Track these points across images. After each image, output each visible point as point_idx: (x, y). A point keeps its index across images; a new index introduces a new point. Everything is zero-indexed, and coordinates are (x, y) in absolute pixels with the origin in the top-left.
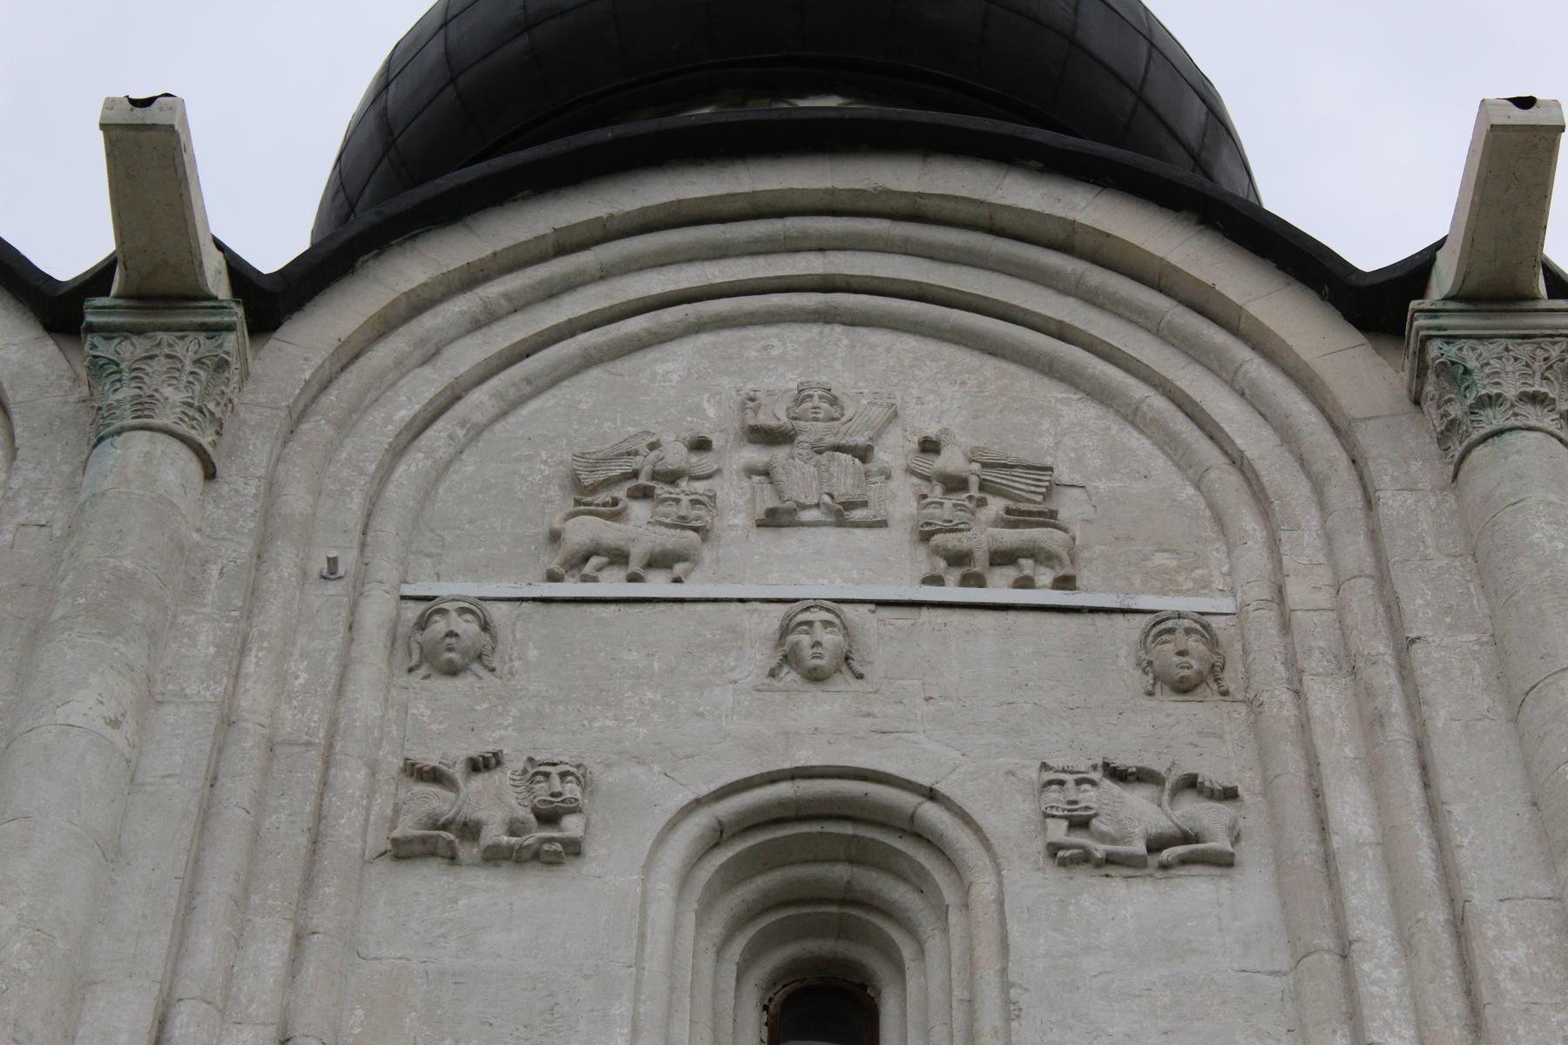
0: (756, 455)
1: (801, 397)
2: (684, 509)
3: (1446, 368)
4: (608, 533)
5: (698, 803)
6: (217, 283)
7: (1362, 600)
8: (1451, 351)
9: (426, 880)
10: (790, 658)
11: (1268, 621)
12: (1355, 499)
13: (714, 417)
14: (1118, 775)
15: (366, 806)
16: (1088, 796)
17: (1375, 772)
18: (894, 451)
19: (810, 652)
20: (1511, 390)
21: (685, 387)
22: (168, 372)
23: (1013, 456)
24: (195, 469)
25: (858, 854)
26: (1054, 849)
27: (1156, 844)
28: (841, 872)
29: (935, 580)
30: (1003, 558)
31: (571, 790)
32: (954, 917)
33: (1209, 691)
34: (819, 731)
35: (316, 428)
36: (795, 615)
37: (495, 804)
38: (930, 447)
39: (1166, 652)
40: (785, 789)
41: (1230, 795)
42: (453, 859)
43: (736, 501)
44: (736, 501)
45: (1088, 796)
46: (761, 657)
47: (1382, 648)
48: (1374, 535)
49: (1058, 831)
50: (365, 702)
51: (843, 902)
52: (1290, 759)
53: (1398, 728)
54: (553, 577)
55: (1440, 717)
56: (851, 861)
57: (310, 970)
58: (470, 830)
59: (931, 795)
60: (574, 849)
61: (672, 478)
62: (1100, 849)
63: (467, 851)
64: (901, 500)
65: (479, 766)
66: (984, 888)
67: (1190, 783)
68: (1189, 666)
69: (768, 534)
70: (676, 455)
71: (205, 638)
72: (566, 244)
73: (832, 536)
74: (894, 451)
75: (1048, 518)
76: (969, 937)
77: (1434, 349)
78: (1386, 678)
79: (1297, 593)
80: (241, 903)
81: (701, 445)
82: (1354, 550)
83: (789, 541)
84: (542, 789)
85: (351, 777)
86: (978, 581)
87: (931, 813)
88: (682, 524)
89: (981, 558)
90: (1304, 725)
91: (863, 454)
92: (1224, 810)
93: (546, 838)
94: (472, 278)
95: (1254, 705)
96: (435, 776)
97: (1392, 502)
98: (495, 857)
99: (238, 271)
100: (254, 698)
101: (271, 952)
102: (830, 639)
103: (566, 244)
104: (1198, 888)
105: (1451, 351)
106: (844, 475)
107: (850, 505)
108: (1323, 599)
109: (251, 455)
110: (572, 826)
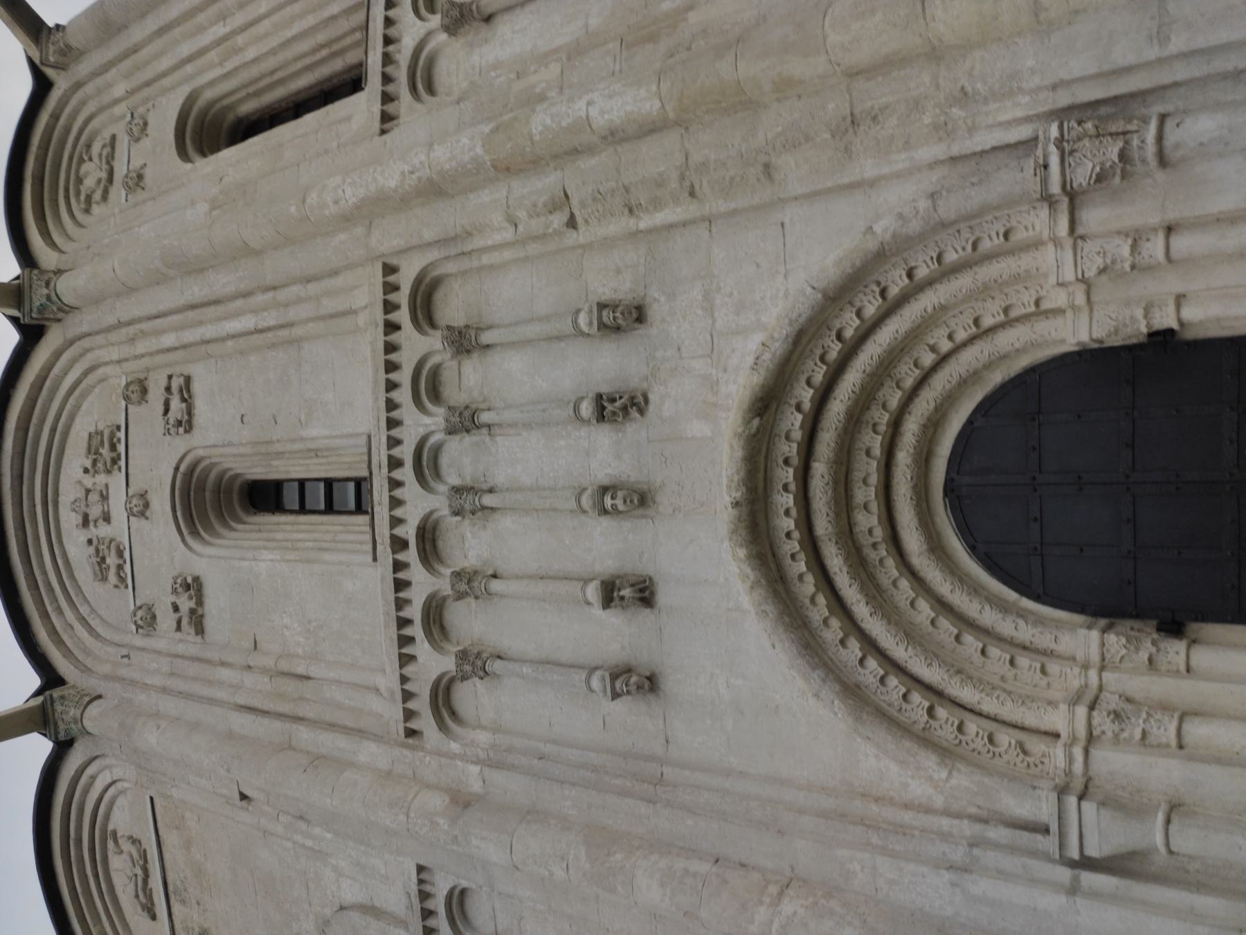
0: (92, 524)
1: (74, 510)
2: (104, 547)
3: (39, 312)
4: (113, 571)
5: (183, 540)
6: (40, 699)
7: (113, 337)
8: (35, 310)
9: (209, 623)
10: (142, 514)
11: (125, 365)
12: (87, 339)
13: (82, 536)
14: (166, 411)
15: (189, 643)
16: (171, 421)
17: (159, 333)
18: (88, 481)
19: (141, 508)
20: (45, 291)
21: (76, 545)
22: (67, 713)
23: (85, 445)
24: (95, 703)
25: (201, 488)
26: (186, 431)
27: (184, 400)
28: (208, 495)
29: (120, 469)
30: (113, 447)
31: (179, 581)
32: (213, 460)
33: (146, 383)
34: (161, 503)
35: (89, 662)
36: (131, 513)
37: (186, 604)
38: (86, 471)
39: (134, 397)
40: (179, 514)
41: (170, 377)
42: (202, 616)
43: (103, 531)
44: (103, 531)
45: (171, 421)
46: (143, 521)
47: (124, 331)
48: (98, 333)
49: (181, 430)
50: (160, 644)
51: (219, 492)
52: (159, 359)
53: (144, 326)
54: (127, 587)
55: (137, 313)
56: (204, 490)
57: (230, 660)
58: (192, 612)
59: (177, 469)
60: (197, 579)
61: (97, 550)
62: (186, 417)
63: (200, 612)
64: (101, 479)
65: (176, 608)
66: (201, 452)
67: (168, 389)
68: (138, 390)
69: (112, 520)
70: (92, 550)
71: (141, 697)
72: (34, 586)
73: (111, 501)
74: (88, 481)
75: (102, 433)
76: (221, 456)
77: (34, 315)
78: (131, 330)
79: (115, 357)
80: (211, 683)
81: (90, 542)
82: (99, 339)
83: (113, 514)
84: (180, 590)
85: (180, 648)
86: (119, 455)
87: (182, 468)
88: (109, 548)
89: (114, 455)
90: (151, 354)
91: (88, 491)
92: (174, 379)
93: (193, 587)
94: (45, 616)
95: (148, 370)
96: (179, 622)
97: (85, 328)
98: (200, 602)
99: (38, 693)
100: (157, 681)
101: (224, 674)
102: (135, 501)
103: (34, 586)
104: (196, 387)
105: (35, 310)
106: (94, 497)
107: (102, 495)
108: (116, 348)
109: (92, 684)
110: (189, 580)
